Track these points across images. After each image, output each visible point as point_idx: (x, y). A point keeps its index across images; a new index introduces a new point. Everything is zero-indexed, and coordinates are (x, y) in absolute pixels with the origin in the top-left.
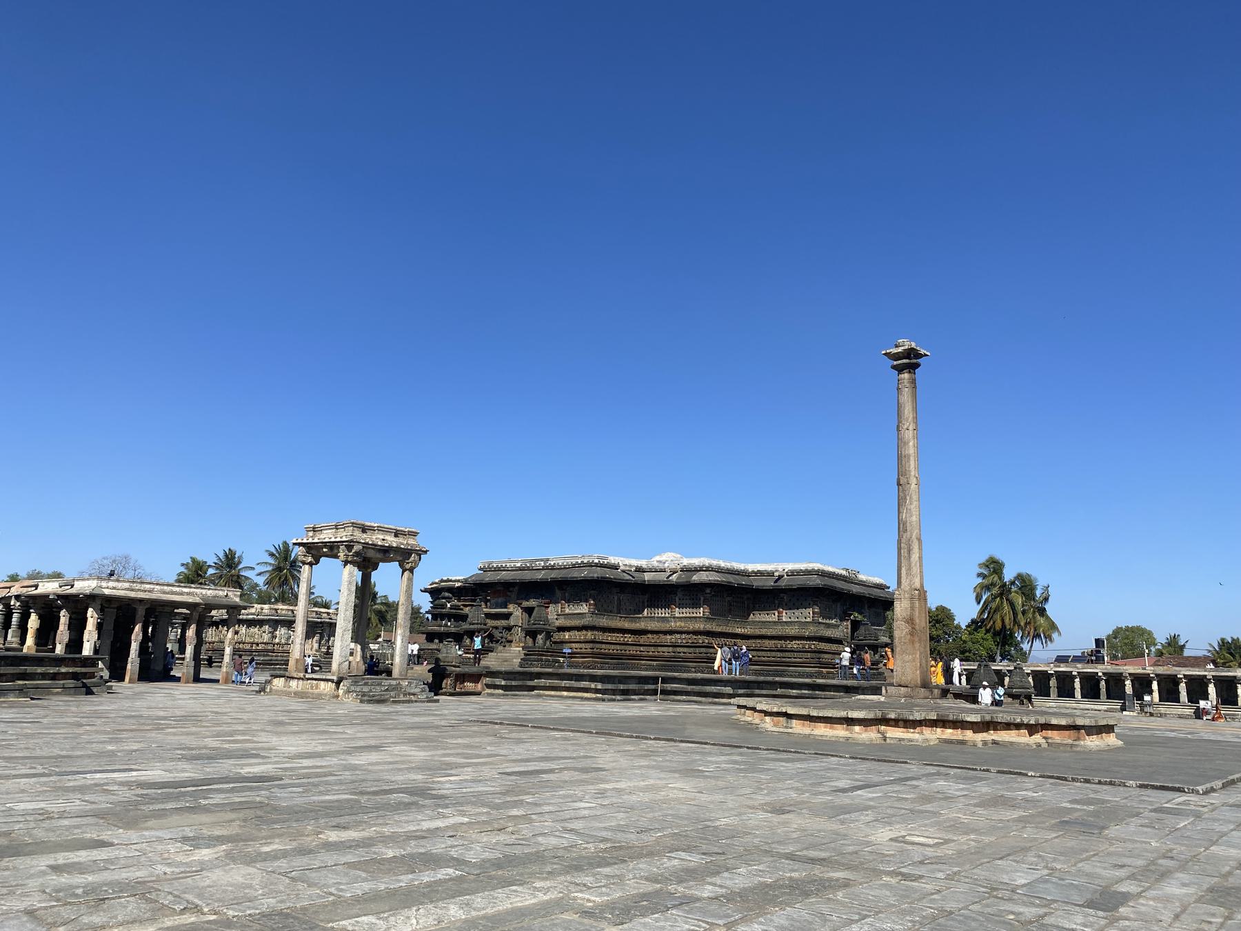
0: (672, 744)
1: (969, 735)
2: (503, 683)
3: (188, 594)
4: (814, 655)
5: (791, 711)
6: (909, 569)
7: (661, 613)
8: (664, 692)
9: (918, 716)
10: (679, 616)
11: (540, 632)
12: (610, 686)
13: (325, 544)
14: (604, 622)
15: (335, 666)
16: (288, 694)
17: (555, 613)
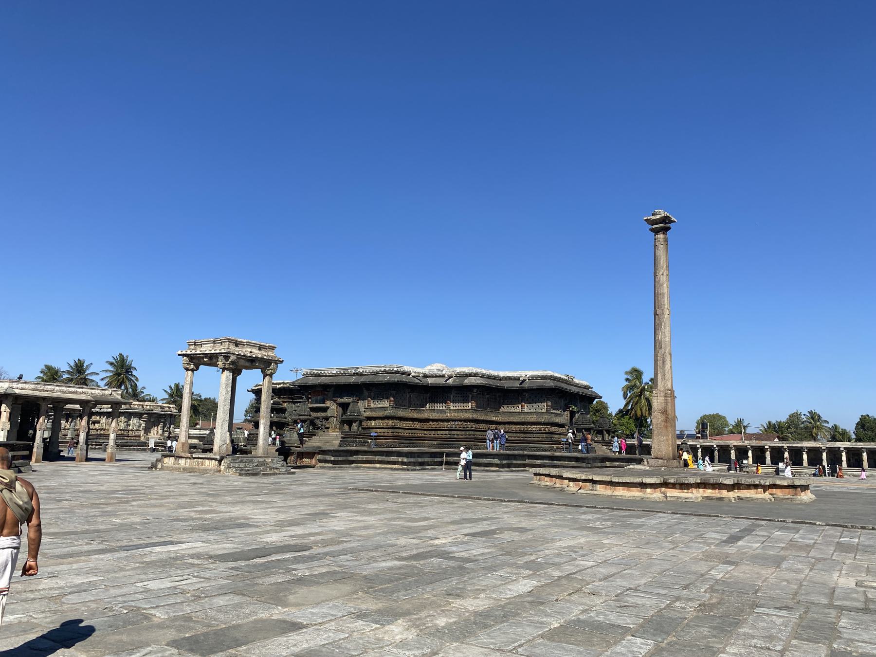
0: (526, 505)
1: (724, 493)
2: (332, 459)
3: (81, 393)
4: (547, 435)
5: (596, 478)
6: (664, 375)
7: (439, 406)
8: (448, 463)
9: (692, 480)
10: (453, 409)
11: (355, 421)
12: (412, 460)
13: (206, 355)
14: (401, 413)
15: (216, 448)
16: (178, 470)
17: (364, 407)
